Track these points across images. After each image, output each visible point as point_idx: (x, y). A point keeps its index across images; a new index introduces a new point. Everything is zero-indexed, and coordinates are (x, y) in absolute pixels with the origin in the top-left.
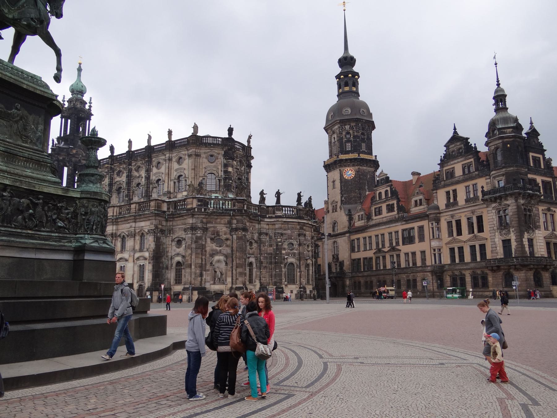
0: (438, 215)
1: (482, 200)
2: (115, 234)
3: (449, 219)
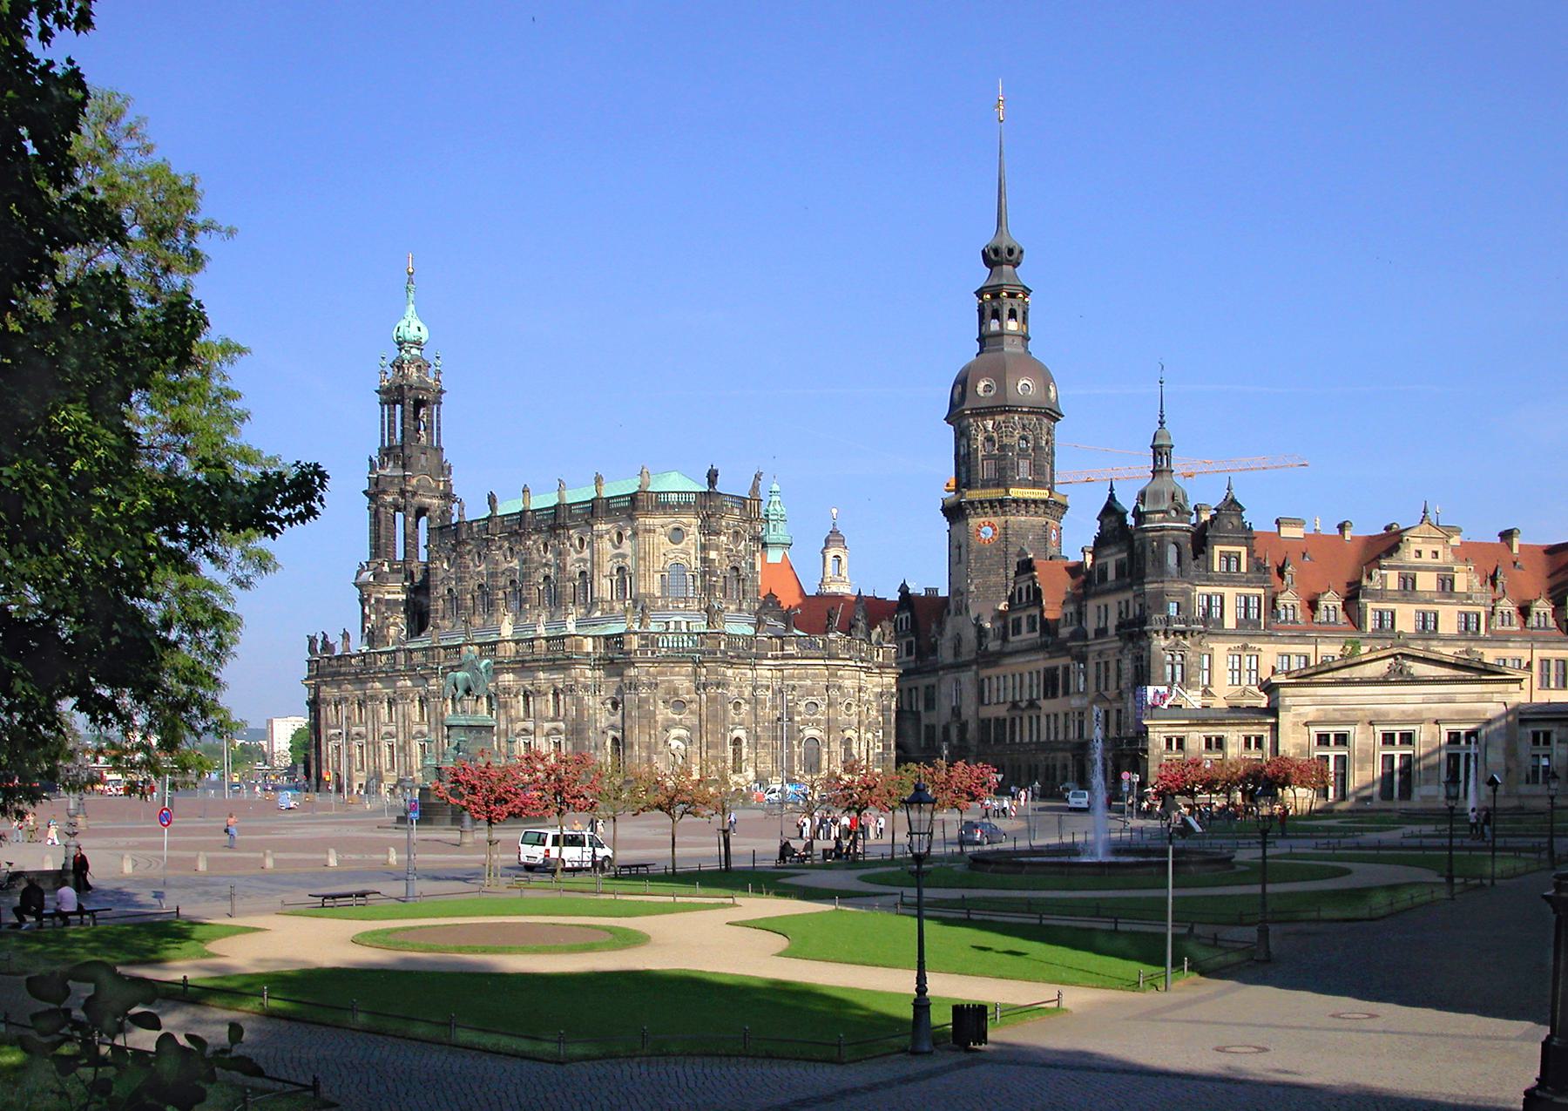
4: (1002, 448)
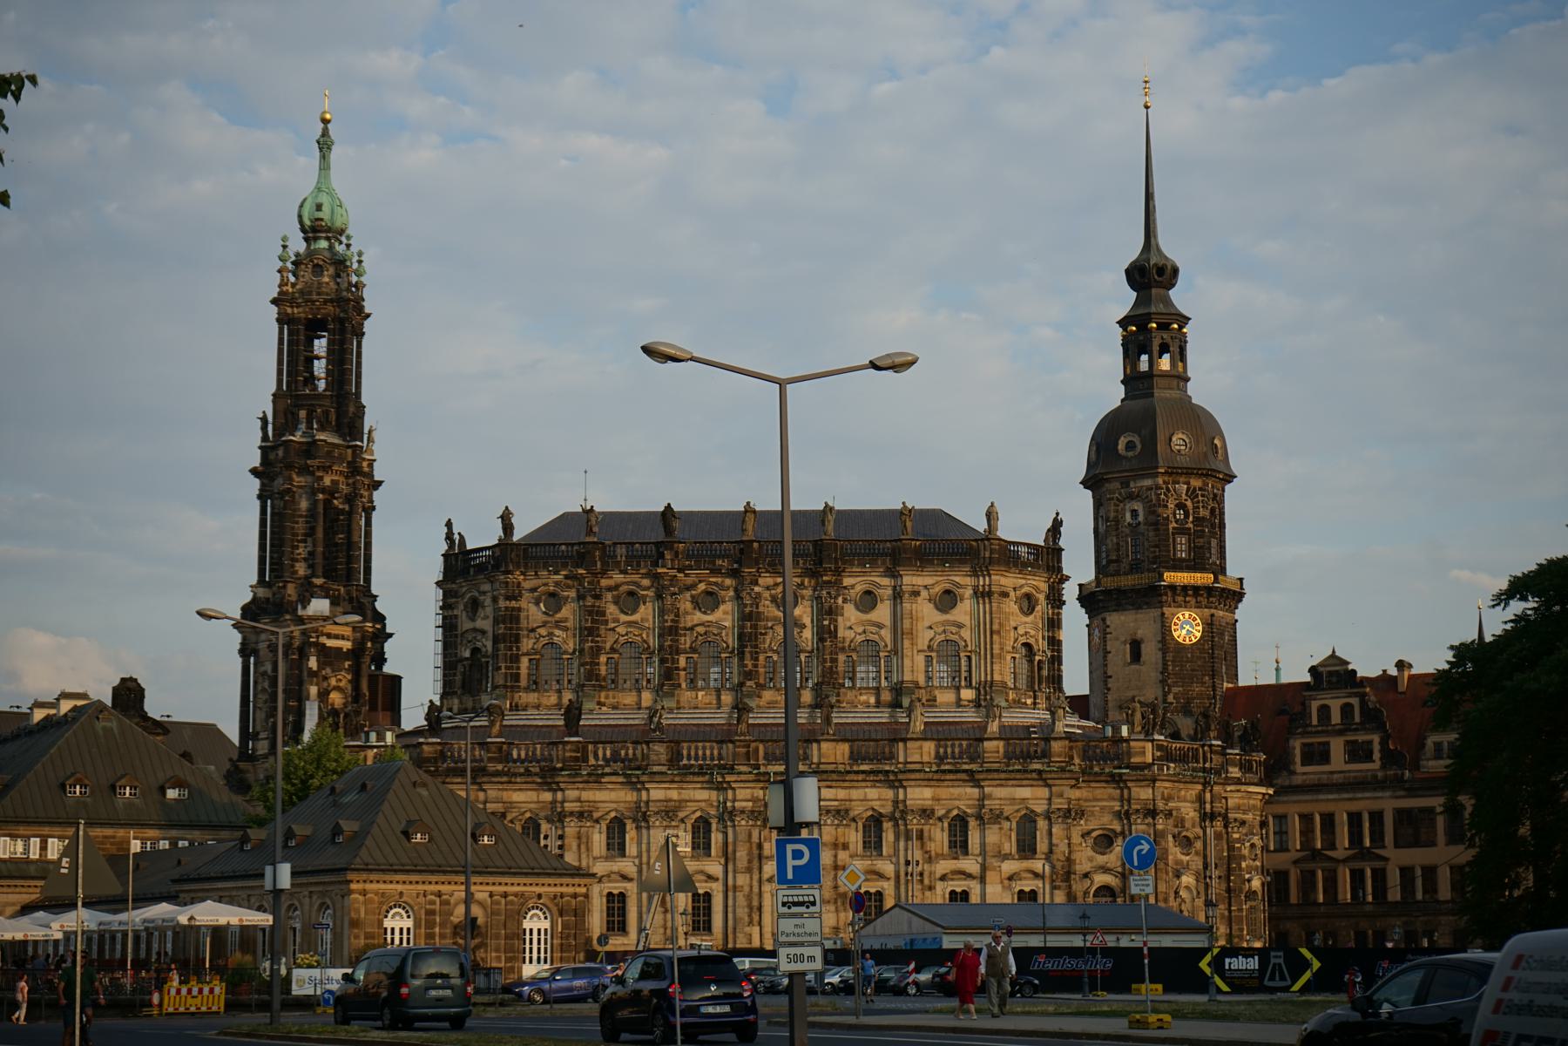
2: (933, 811)
4: (1198, 520)
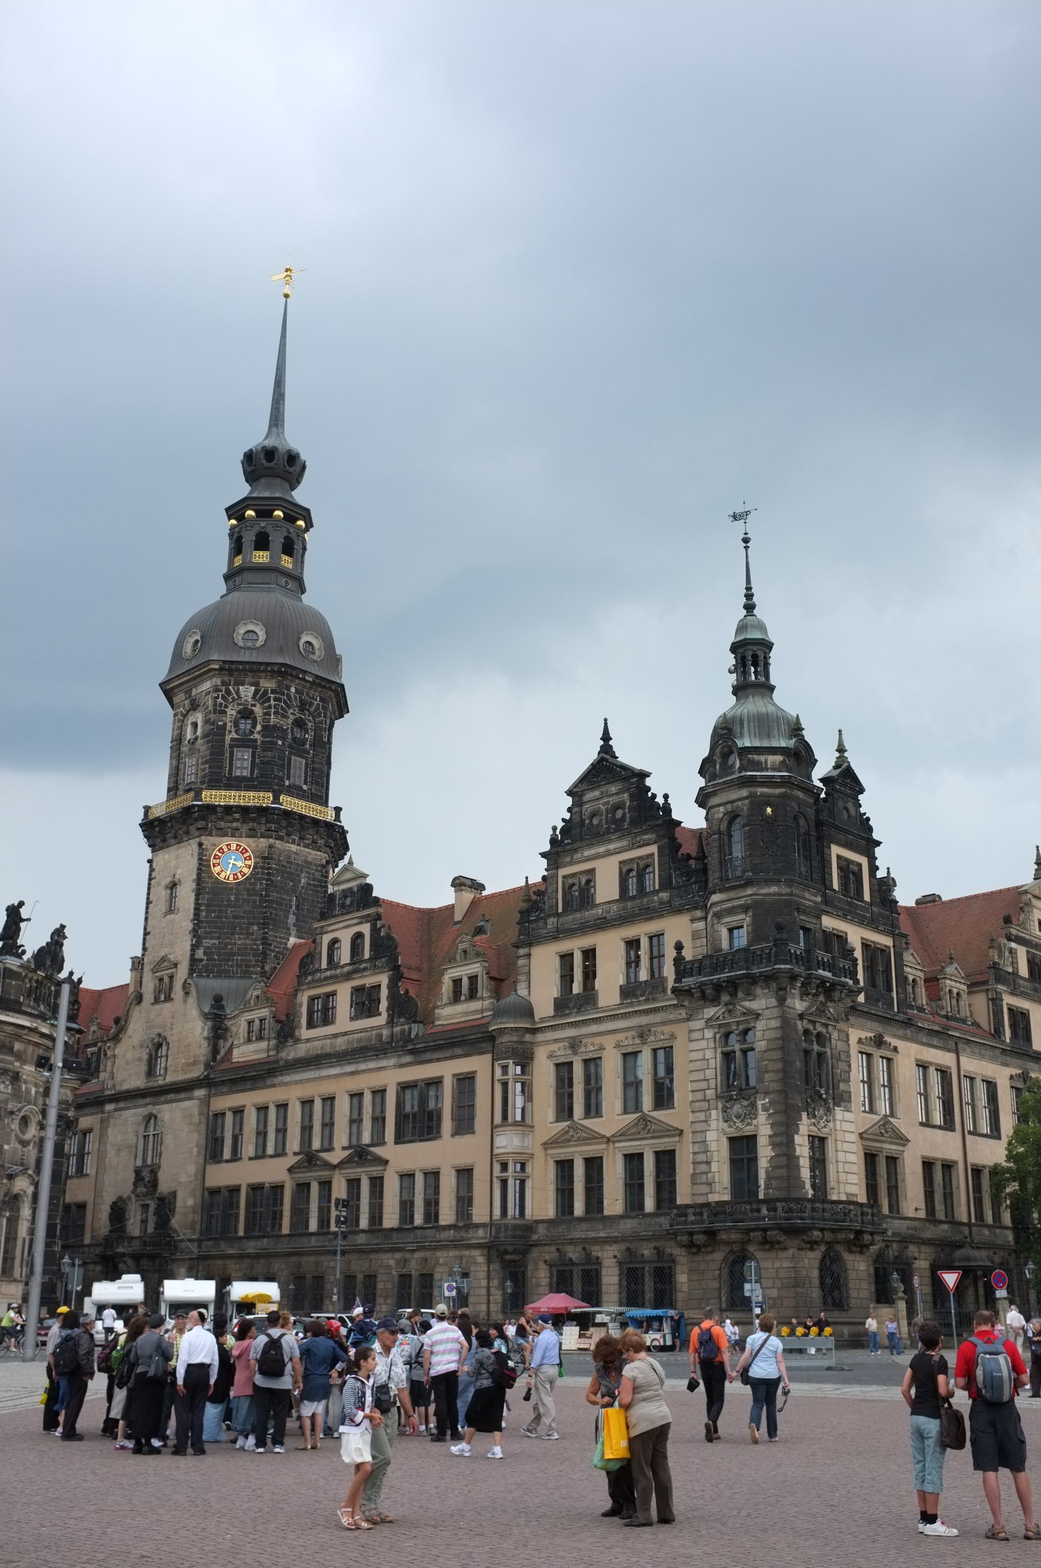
0: (528, 1037)
1: (674, 990)
3: (563, 1054)
